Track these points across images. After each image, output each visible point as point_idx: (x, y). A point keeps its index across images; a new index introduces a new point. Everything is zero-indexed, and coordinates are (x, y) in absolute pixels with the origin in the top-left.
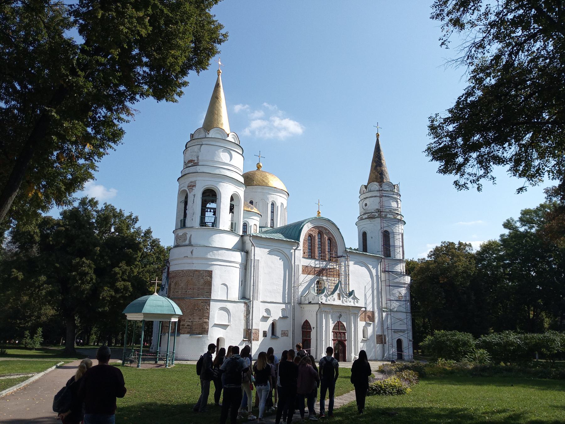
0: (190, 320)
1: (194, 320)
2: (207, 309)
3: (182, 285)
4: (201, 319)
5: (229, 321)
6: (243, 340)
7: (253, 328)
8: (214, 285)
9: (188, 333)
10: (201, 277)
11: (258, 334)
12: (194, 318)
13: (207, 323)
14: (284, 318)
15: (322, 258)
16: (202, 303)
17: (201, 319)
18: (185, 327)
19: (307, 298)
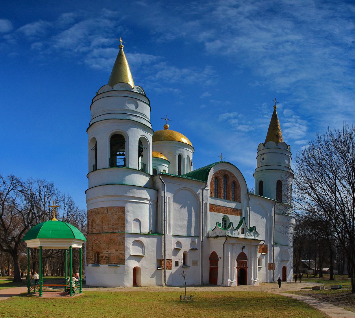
0: (108, 252)
1: (111, 252)
2: (123, 242)
3: (98, 221)
4: (117, 251)
5: (143, 252)
6: (158, 269)
7: (166, 259)
8: (127, 221)
9: (107, 263)
10: (114, 213)
11: (170, 264)
12: (111, 250)
13: (124, 255)
14: (193, 250)
15: (227, 198)
16: (117, 237)
17: (117, 251)
18: (103, 258)
19: (214, 232)
